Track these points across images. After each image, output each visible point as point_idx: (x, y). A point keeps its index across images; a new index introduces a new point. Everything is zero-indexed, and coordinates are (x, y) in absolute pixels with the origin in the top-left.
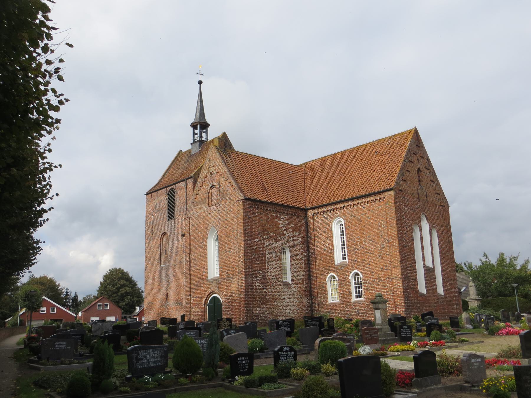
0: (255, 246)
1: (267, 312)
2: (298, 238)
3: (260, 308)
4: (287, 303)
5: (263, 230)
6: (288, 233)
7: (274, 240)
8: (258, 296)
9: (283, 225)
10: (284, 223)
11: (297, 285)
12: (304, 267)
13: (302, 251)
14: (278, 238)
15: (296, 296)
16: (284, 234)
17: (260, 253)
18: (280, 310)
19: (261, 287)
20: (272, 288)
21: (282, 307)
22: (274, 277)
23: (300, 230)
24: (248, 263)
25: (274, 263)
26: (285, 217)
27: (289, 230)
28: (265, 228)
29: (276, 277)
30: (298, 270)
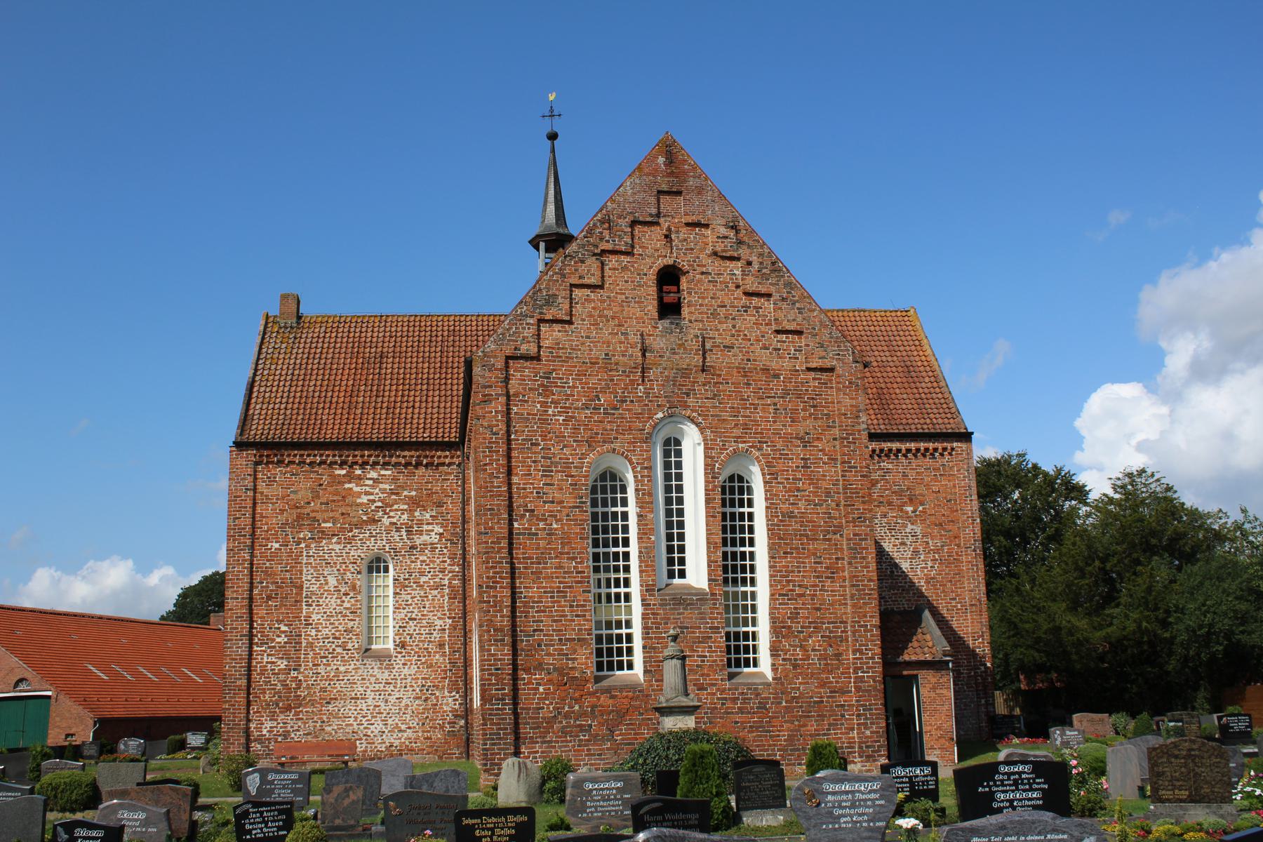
0: (268, 560)
1: (298, 731)
2: (430, 527)
3: (276, 720)
4: (375, 706)
5: (299, 517)
6: (389, 517)
7: (335, 540)
8: (268, 689)
9: (372, 497)
10: (377, 491)
11: (416, 658)
12: (446, 604)
13: (445, 562)
14: (350, 534)
15: (412, 686)
16: (374, 521)
17: (281, 579)
18: (347, 725)
19: (282, 666)
20: (321, 669)
21: (356, 718)
22: (328, 638)
23: (440, 505)
24: (236, 606)
25: (333, 601)
26: (383, 472)
27: (396, 507)
28: (306, 511)
29: (333, 638)
30: (423, 615)
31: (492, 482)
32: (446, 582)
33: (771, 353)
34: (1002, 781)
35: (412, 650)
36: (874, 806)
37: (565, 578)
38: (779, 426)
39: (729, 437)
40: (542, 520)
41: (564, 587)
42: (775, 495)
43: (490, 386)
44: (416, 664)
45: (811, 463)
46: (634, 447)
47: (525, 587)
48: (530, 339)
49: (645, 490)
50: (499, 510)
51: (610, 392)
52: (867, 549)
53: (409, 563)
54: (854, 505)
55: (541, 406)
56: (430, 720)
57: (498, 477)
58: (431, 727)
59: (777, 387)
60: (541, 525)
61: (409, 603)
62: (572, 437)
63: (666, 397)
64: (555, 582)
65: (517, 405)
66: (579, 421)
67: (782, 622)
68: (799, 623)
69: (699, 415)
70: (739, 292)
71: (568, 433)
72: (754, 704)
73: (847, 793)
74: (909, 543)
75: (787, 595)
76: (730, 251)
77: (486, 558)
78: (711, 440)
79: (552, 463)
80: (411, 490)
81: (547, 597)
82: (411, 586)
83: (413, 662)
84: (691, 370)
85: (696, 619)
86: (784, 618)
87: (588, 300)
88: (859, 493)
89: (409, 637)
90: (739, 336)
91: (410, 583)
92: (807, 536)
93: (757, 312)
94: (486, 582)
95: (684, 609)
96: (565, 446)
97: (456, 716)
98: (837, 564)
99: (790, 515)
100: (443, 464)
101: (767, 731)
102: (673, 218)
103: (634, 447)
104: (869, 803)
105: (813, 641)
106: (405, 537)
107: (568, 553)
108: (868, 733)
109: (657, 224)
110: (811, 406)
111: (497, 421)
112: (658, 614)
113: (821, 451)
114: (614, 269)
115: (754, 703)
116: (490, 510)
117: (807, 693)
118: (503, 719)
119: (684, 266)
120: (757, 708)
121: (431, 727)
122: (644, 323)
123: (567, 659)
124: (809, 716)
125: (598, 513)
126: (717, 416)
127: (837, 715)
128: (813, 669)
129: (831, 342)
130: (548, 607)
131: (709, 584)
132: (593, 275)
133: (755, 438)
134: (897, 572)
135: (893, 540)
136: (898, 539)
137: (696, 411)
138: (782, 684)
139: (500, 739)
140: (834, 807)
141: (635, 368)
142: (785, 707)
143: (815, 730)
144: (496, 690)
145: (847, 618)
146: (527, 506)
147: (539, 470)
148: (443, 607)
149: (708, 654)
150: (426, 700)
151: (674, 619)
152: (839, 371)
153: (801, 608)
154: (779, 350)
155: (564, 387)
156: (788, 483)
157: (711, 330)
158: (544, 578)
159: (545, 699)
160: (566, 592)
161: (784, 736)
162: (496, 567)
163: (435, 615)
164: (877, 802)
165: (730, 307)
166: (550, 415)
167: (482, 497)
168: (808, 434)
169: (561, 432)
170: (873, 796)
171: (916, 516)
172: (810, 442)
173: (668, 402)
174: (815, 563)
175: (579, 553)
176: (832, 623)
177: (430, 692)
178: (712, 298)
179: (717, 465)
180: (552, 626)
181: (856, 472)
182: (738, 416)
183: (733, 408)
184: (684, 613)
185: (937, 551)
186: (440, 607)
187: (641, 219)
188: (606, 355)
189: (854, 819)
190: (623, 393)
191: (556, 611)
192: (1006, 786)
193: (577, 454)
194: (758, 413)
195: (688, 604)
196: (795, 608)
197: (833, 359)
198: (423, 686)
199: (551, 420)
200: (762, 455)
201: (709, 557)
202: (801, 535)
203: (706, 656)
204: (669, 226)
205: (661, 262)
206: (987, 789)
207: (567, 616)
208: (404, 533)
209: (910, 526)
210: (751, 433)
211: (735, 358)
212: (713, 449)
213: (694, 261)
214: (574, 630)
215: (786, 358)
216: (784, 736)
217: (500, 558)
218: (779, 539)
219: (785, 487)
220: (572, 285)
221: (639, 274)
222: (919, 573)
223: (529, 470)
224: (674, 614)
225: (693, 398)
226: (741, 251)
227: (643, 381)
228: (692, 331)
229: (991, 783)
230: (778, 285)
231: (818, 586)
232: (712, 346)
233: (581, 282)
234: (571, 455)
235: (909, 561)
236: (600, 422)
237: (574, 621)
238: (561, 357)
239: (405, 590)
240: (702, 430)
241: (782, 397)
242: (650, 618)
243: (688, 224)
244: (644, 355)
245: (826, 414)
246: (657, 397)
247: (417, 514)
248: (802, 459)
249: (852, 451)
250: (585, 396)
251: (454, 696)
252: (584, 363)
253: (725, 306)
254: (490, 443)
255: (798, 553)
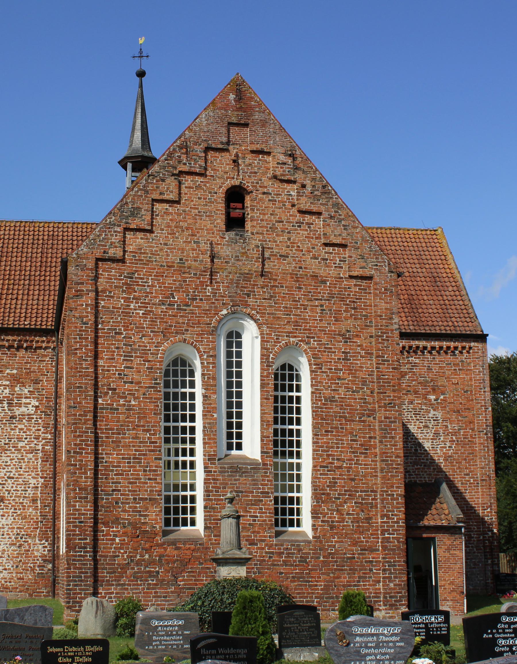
2: (28, 401)
11: (12, 510)
12: (39, 466)
13: (40, 430)
15: (8, 534)
23: (36, 382)
30: (19, 475)
31: (82, 364)
32: (40, 447)
33: (319, 263)
34: (504, 629)
35: (10, 503)
36: (395, 647)
37: (140, 447)
38: (324, 324)
39: (282, 332)
40: (122, 397)
41: (139, 455)
42: (320, 382)
43: (82, 283)
44: (13, 516)
45: (350, 356)
46: (202, 338)
47: (106, 454)
48: (117, 244)
49: (210, 374)
50: (86, 388)
51: (182, 291)
52: (395, 430)
53: (9, 430)
54: (385, 393)
55: (124, 302)
56: (23, 564)
57: (87, 360)
58: (23, 570)
59: (324, 291)
60: (122, 402)
61: (8, 464)
62: (150, 328)
63: (230, 297)
64: (132, 450)
65: (104, 300)
66: (155, 315)
67: (322, 490)
68: (336, 490)
69: (257, 312)
70: (295, 210)
71: (146, 324)
72: (296, 558)
73: (372, 635)
74: (431, 426)
75: (327, 467)
76: (287, 175)
77: (74, 428)
78: (267, 334)
79: (132, 349)
80: (13, 369)
81: (125, 463)
82: (10, 450)
83: (10, 514)
84: (252, 274)
85: (250, 484)
86: (324, 486)
87: (167, 213)
88: (390, 383)
89: (7, 493)
90: (293, 247)
91: (9, 447)
92: (345, 417)
93: (309, 227)
94: (74, 449)
95: (240, 476)
96: (143, 336)
97: (45, 561)
98: (370, 442)
99: (332, 400)
100: (40, 348)
101: (307, 581)
102: (240, 146)
103: (202, 338)
104: (391, 644)
105: (348, 507)
106: (6, 408)
107: (143, 426)
108: (392, 585)
109: (227, 150)
110: (352, 308)
111: (87, 312)
112: (217, 480)
113: (359, 346)
114: (190, 187)
115: (296, 557)
116: (79, 387)
117: (342, 550)
118: (84, 564)
119: (248, 186)
120: (299, 561)
121: (23, 570)
122: (213, 233)
123: (140, 515)
124: (342, 570)
125: (169, 393)
126: (272, 314)
127: (366, 570)
128: (347, 530)
129: (370, 254)
130: (125, 471)
131: (262, 456)
132: (172, 192)
133: (304, 333)
134: (421, 450)
135: (417, 423)
136: (422, 422)
137: (255, 309)
138: (321, 542)
139: (81, 581)
140: (361, 647)
141: (204, 271)
142: (323, 561)
143: (347, 582)
144: (80, 539)
145: (377, 488)
146: (110, 385)
147: (121, 355)
148: (37, 468)
149: (259, 515)
150: (20, 546)
151: (231, 484)
152: (377, 279)
153: (338, 479)
154: (327, 260)
155: (144, 286)
156: (331, 373)
157: (269, 241)
158: (123, 446)
159: (121, 548)
160: (141, 459)
161: (321, 585)
162: (82, 436)
163: (30, 475)
164: (398, 644)
165: (286, 222)
166: (131, 309)
167: (72, 376)
168: (348, 331)
169: (140, 324)
170: (394, 638)
171: (438, 403)
172: (350, 339)
173: (232, 301)
174: (351, 440)
175: (152, 426)
176: (365, 491)
177: (23, 540)
178: (271, 214)
179: (271, 356)
180: (128, 487)
181: (388, 365)
182: (290, 315)
183: (286, 308)
184: (239, 480)
185: (454, 434)
186: (34, 468)
187: (213, 146)
188: (181, 260)
189: (378, 658)
190: (194, 292)
191: (132, 474)
192: (507, 633)
193: (154, 343)
194: (308, 313)
195: (243, 472)
196: (334, 478)
197: (372, 269)
198: (18, 534)
199: (133, 313)
200: (309, 348)
201: (262, 433)
202: (340, 417)
203: (257, 517)
204: (237, 153)
205: (229, 183)
206: (491, 636)
207: (141, 479)
208: (5, 405)
209: (432, 412)
210: (300, 330)
211: (289, 265)
212: (268, 342)
213: (257, 183)
214: (147, 491)
215: (332, 267)
216: (321, 585)
217: (86, 428)
218: (322, 419)
219: (328, 376)
220: (154, 200)
221: (210, 193)
222: (439, 451)
223: (113, 355)
224: (231, 480)
225: (253, 298)
226: (297, 176)
227: (211, 283)
228: (254, 242)
229: (494, 631)
230: (327, 205)
231: (353, 460)
232: (270, 255)
233: (161, 197)
234: (149, 343)
235: (430, 441)
236: (174, 316)
237: (147, 483)
238: (142, 260)
239: (5, 453)
240: (259, 326)
241: (328, 300)
242: (211, 483)
243: (253, 152)
244: (212, 261)
245: (364, 316)
246: (222, 296)
247: (17, 389)
248: (343, 352)
249: (385, 347)
250: (161, 294)
251: (44, 544)
252: (161, 266)
253: (282, 222)
254: (80, 331)
255: (337, 432)
